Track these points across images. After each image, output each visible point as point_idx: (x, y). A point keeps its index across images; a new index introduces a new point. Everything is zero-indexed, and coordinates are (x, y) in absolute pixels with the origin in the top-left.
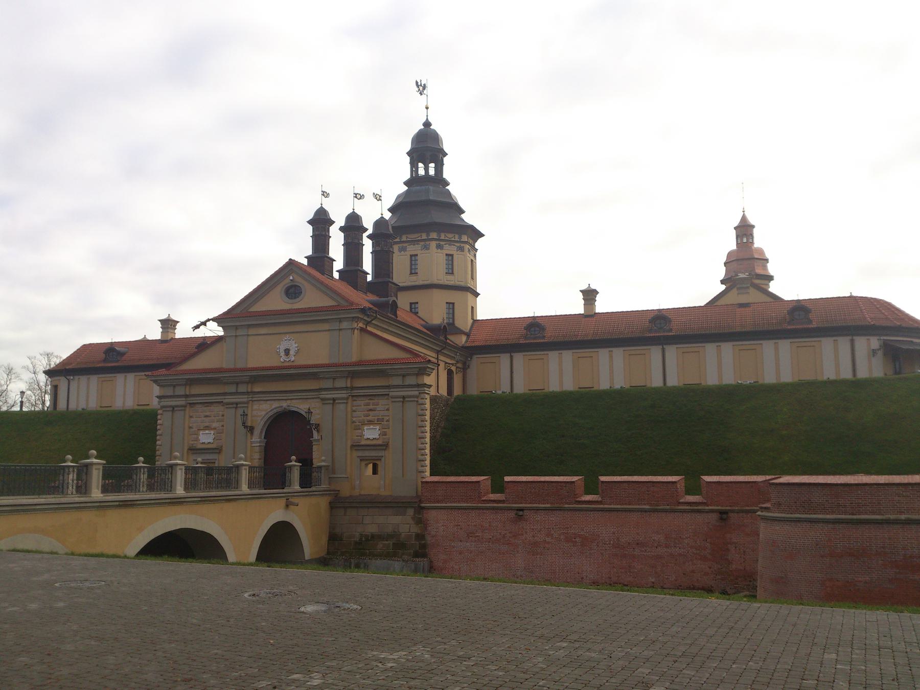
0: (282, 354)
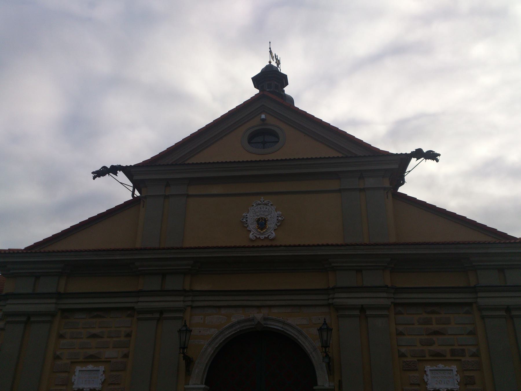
0: (252, 226)
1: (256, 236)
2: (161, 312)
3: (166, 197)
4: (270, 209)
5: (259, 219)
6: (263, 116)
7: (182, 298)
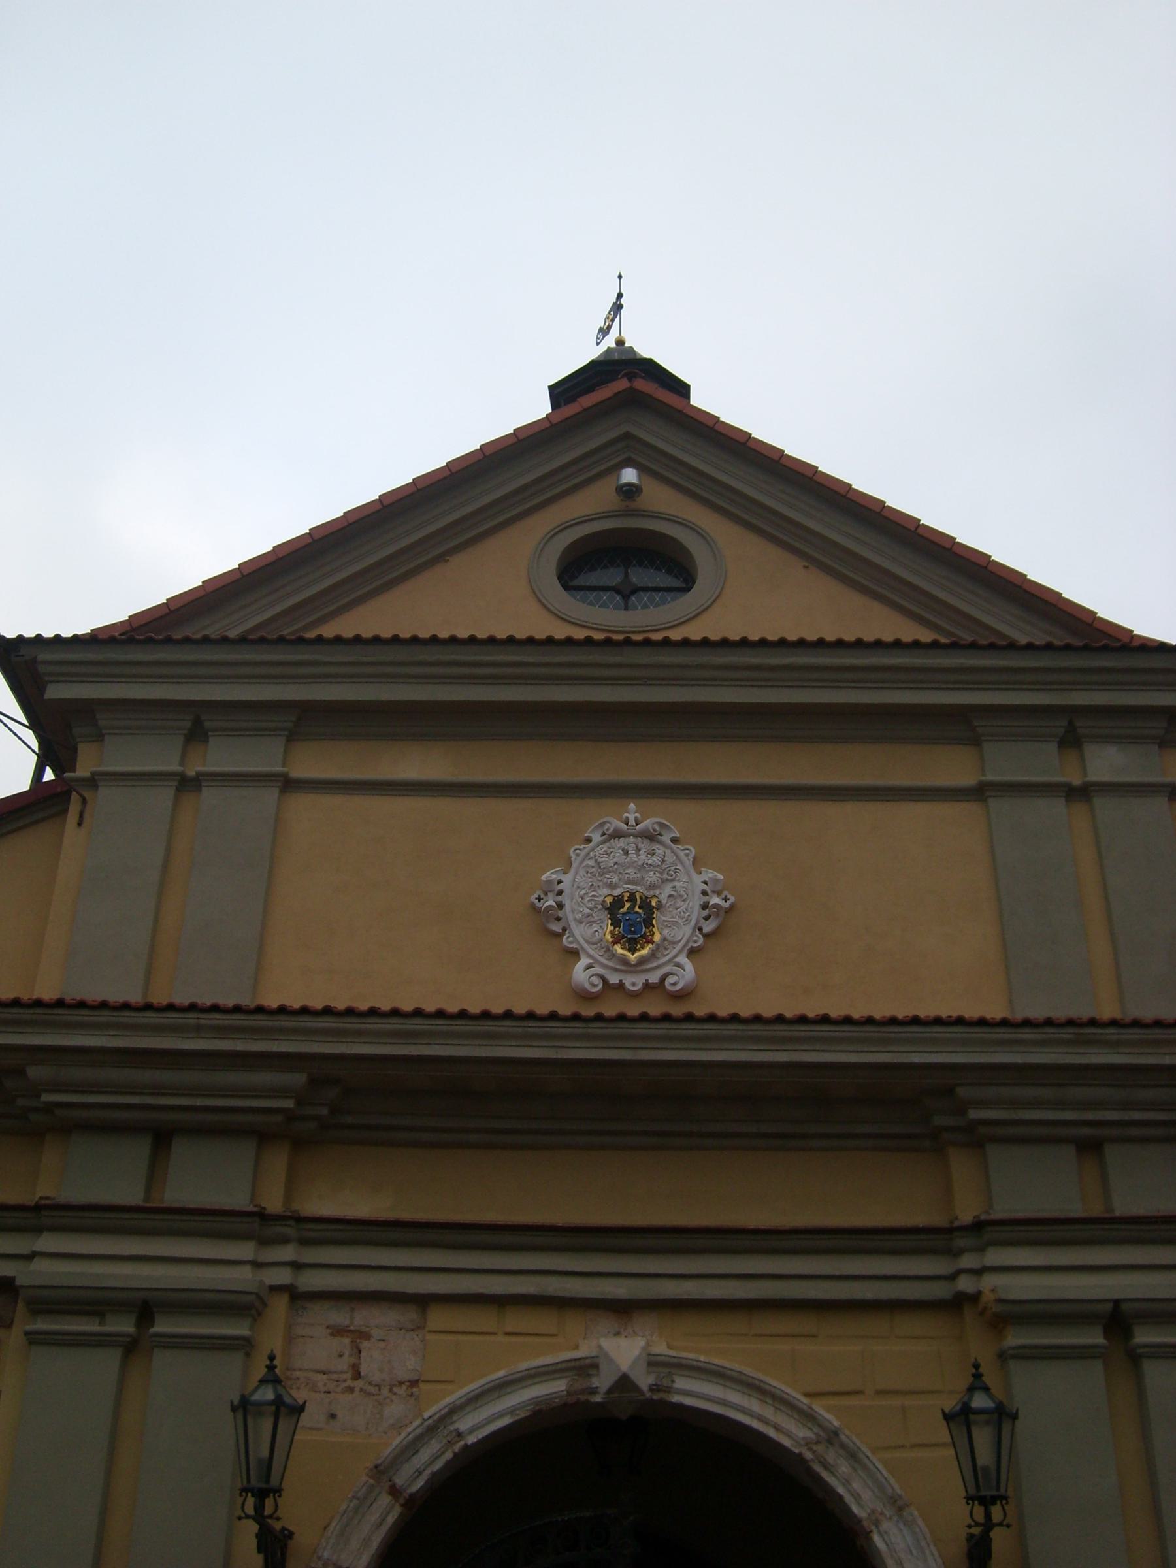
0: (589, 931)
1: (605, 980)
2: (146, 1308)
3: (187, 784)
4: (670, 858)
5: (618, 902)
6: (629, 475)
7: (245, 1250)
